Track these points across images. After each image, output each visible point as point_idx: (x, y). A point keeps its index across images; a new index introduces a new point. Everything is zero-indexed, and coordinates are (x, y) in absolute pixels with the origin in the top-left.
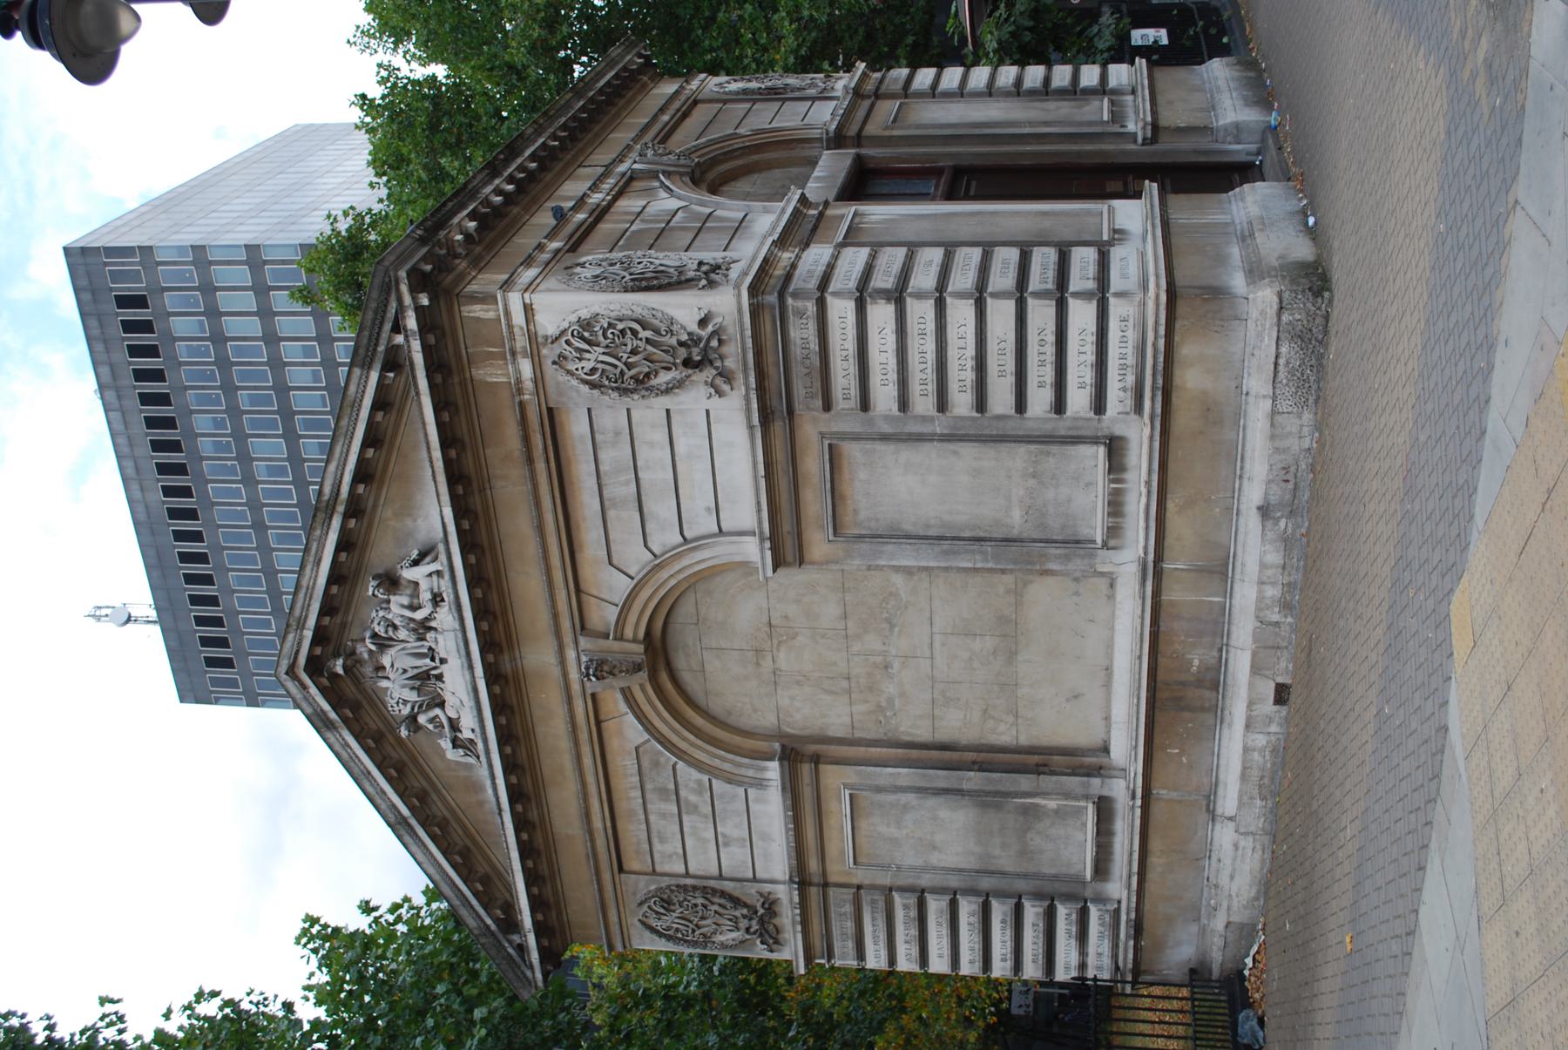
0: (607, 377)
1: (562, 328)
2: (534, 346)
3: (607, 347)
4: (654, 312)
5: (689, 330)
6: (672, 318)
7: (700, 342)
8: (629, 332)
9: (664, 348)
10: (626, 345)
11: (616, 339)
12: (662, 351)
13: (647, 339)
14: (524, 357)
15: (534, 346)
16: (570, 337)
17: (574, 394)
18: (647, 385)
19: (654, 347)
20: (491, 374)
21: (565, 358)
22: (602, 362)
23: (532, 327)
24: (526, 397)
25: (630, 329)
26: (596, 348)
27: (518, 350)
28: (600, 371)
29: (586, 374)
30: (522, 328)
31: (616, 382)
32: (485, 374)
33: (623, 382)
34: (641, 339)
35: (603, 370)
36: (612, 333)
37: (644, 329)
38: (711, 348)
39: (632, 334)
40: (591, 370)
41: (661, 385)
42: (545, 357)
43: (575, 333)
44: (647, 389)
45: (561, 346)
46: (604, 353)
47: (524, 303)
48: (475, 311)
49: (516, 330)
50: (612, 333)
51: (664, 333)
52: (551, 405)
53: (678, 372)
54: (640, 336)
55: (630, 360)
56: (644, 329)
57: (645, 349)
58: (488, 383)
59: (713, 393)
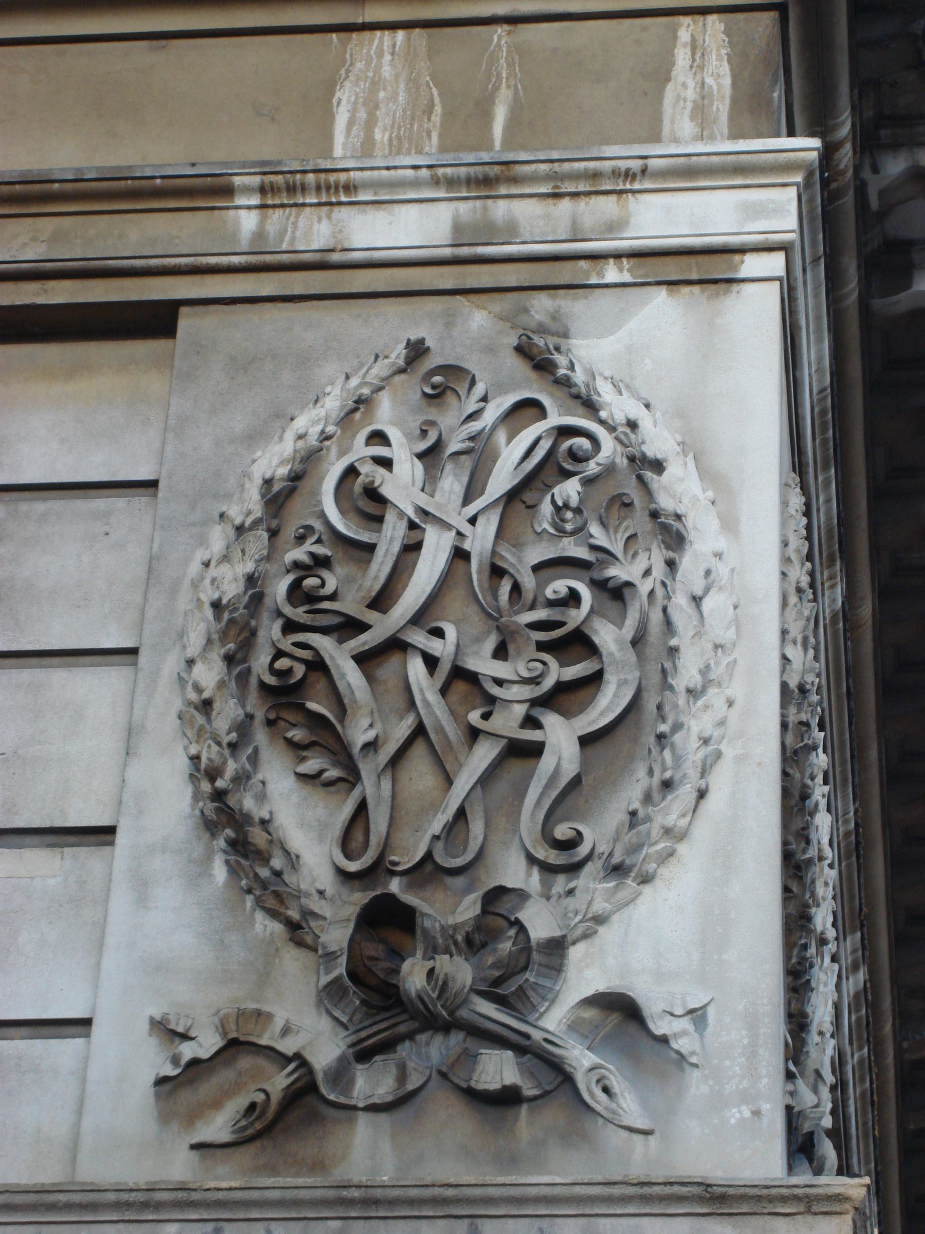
0: (322, 562)
1: (605, 393)
2: (510, 275)
3: (497, 572)
4: (685, 793)
5: (575, 953)
6: (646, 879)
7: (502, 1001)
8: (573, 672)
9: (477, 827)
10: (501, 652)
11: (541, 614)
12: (461, 814)
13: (535, 750)
14: (457, 228)
15: (510, 275)
16: (555, 419)
17: (239, 422)
18: (261, 736)
19: (486, 780)
20: (373, 107)
21: (436, 396)
22: (412, 548)
23: (612, 273)
24: (248, 221)
25: (596, 679)
26: (488, 527)
27: (500, 210)
28: (365, 537)
29: (351, 472)
30: (612, 228)
31: (296, 593)
32: (376, 84)
33: (290, 627)
34: (531, 722)
35: (370, 548)
36: (573, 598)
37: (586, 741)
38: (469, 1058)
39: (562, 688)
40: (373, 494)
41: (262, 797)
42: (450, 320)
43: (583, 443)
44: (243, 728)
45: (502, 388)
46: (460, 555)
47: (742, 250)
48: (698, 66)
49: (607, 206)
50: (573, 598)
51: (562, 831)
52: (186, 322)
53: (326, 879)
54: (551, 720)
55: (416, 668)
56: (586, 741)
57: (474, 734)
58: (330, 87)
59: (188, 1051)
